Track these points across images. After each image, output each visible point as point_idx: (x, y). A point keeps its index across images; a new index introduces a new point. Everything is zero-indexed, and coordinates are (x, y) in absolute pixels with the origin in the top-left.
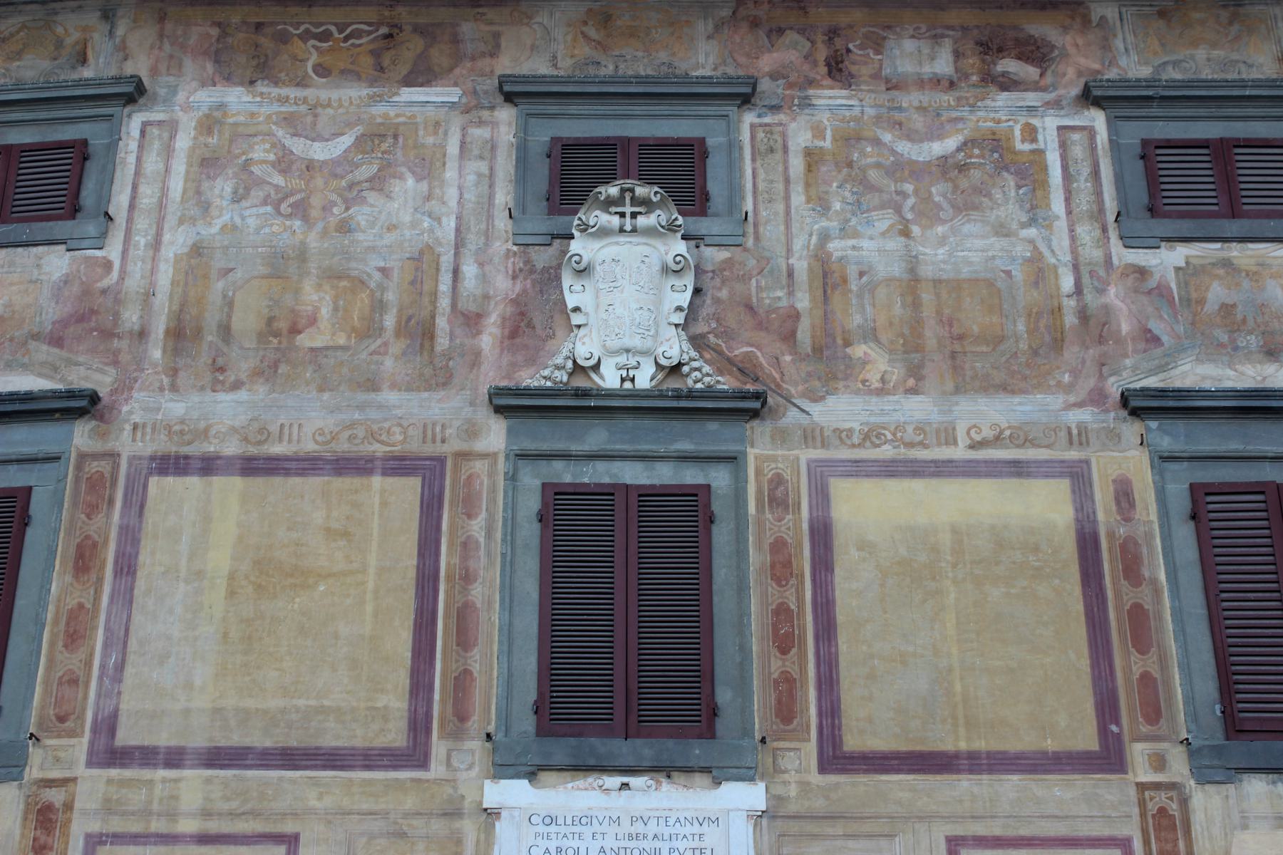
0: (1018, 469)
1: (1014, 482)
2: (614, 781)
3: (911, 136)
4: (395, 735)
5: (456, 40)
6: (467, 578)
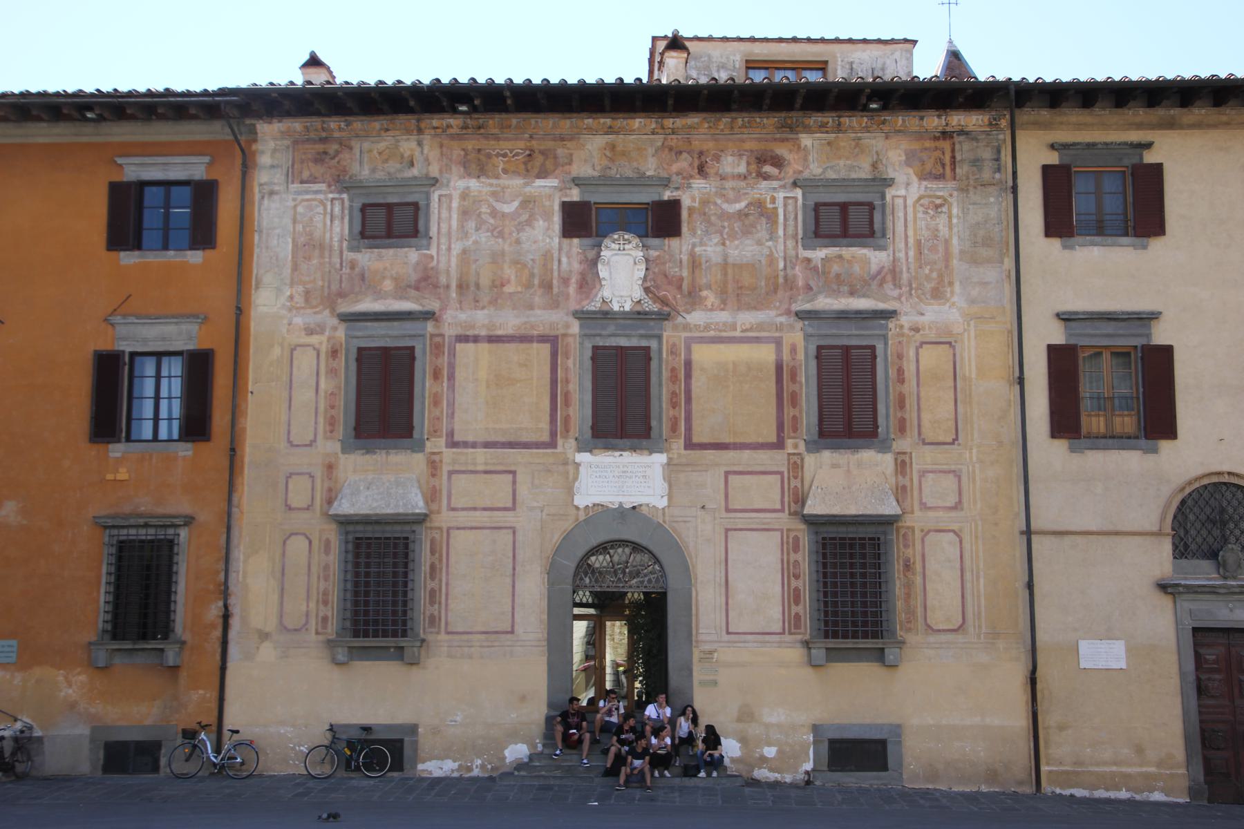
0: (757, 340)
1: (755, 345)
2: (617, 454)
3: (728, 201)
5: (555, 157)
6: (567, 381)
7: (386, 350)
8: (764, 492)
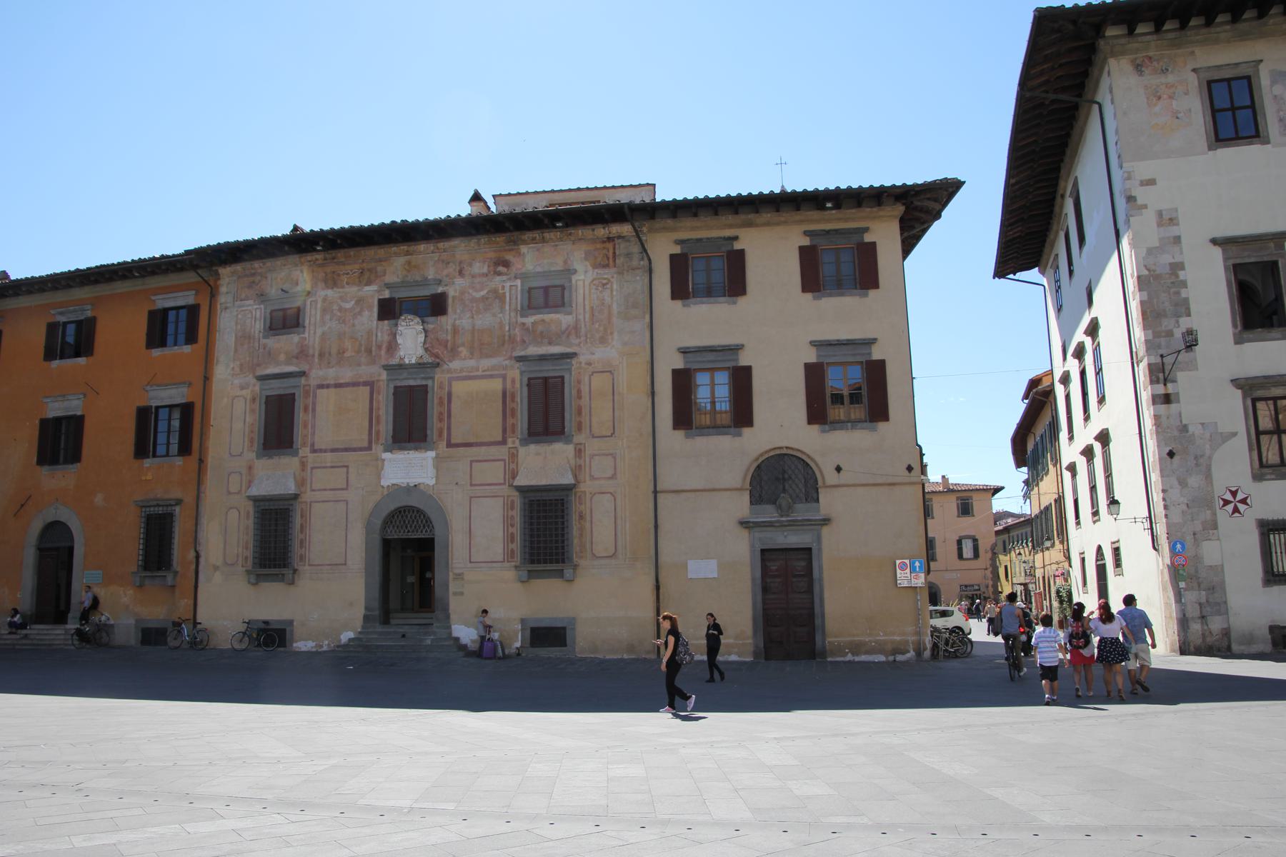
0: (491, 376)
4: (366, 444)
7: (280, 396)
8: (494, 473)
